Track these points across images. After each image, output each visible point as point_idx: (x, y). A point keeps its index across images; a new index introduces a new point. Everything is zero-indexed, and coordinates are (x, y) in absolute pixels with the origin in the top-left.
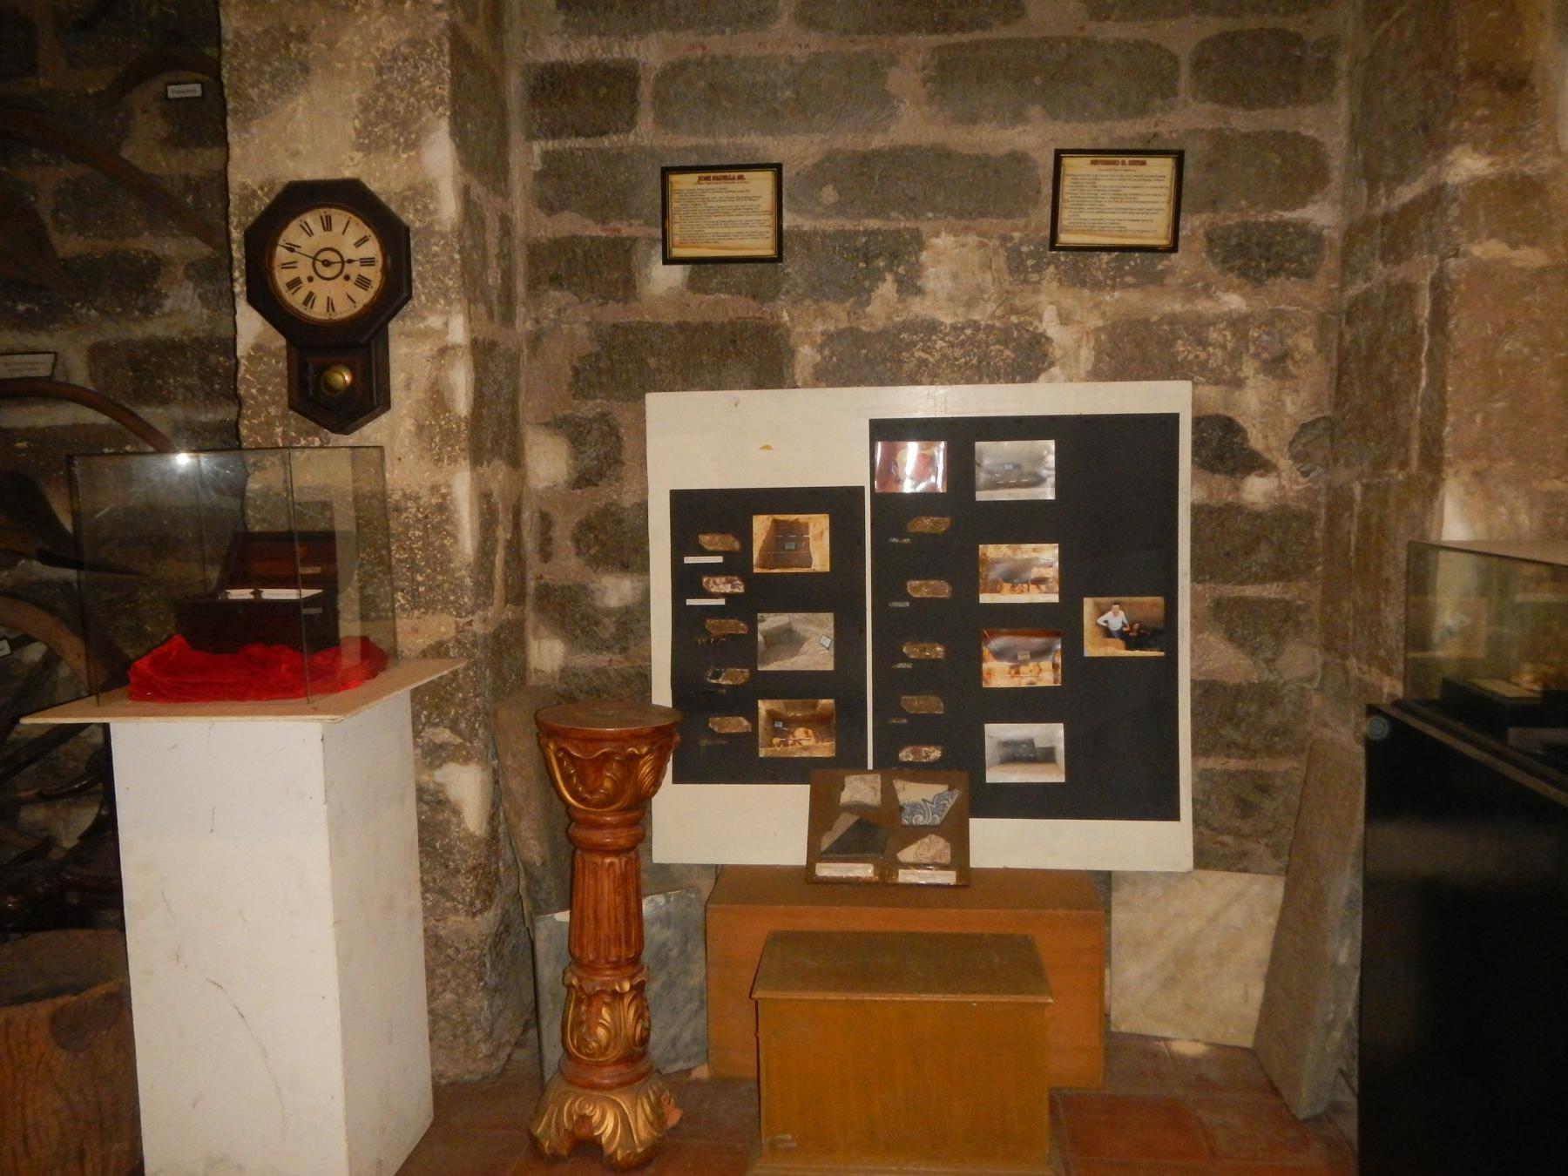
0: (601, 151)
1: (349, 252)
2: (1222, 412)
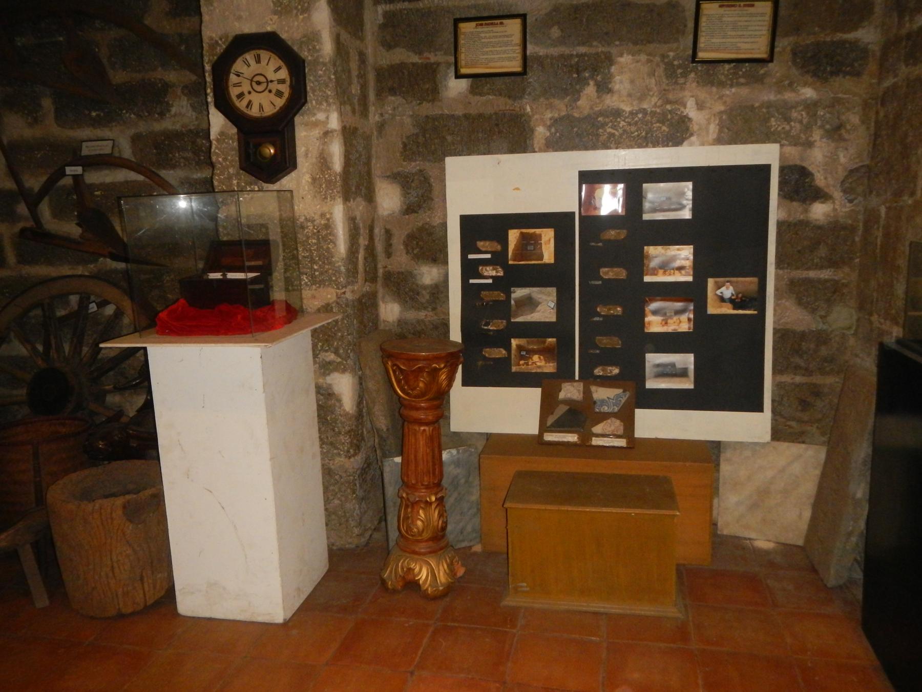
0: (418, 10)
1: (271, 76)
2: (798, 163)
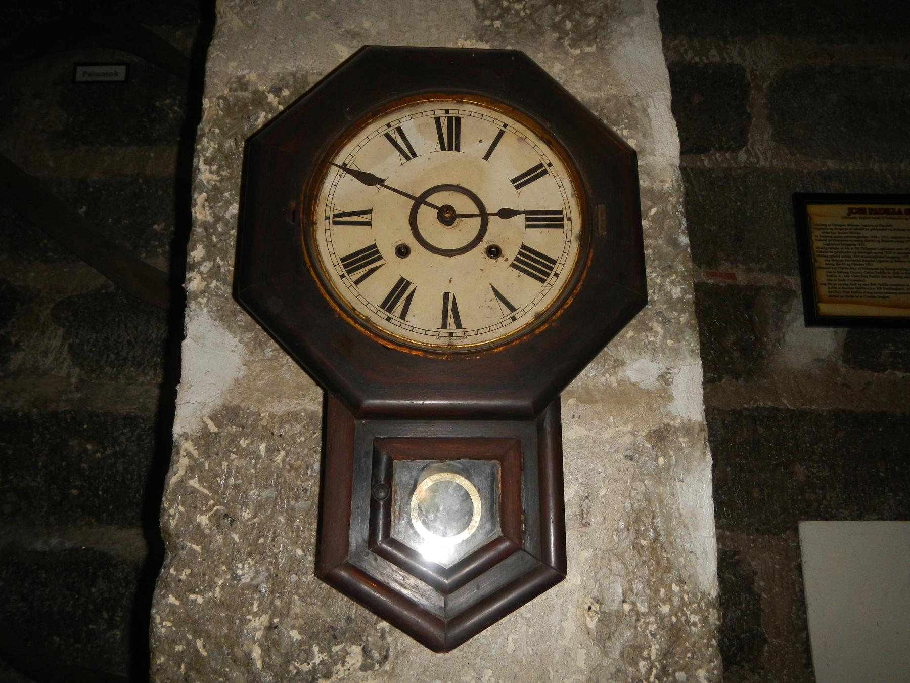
1: (498, 193)
